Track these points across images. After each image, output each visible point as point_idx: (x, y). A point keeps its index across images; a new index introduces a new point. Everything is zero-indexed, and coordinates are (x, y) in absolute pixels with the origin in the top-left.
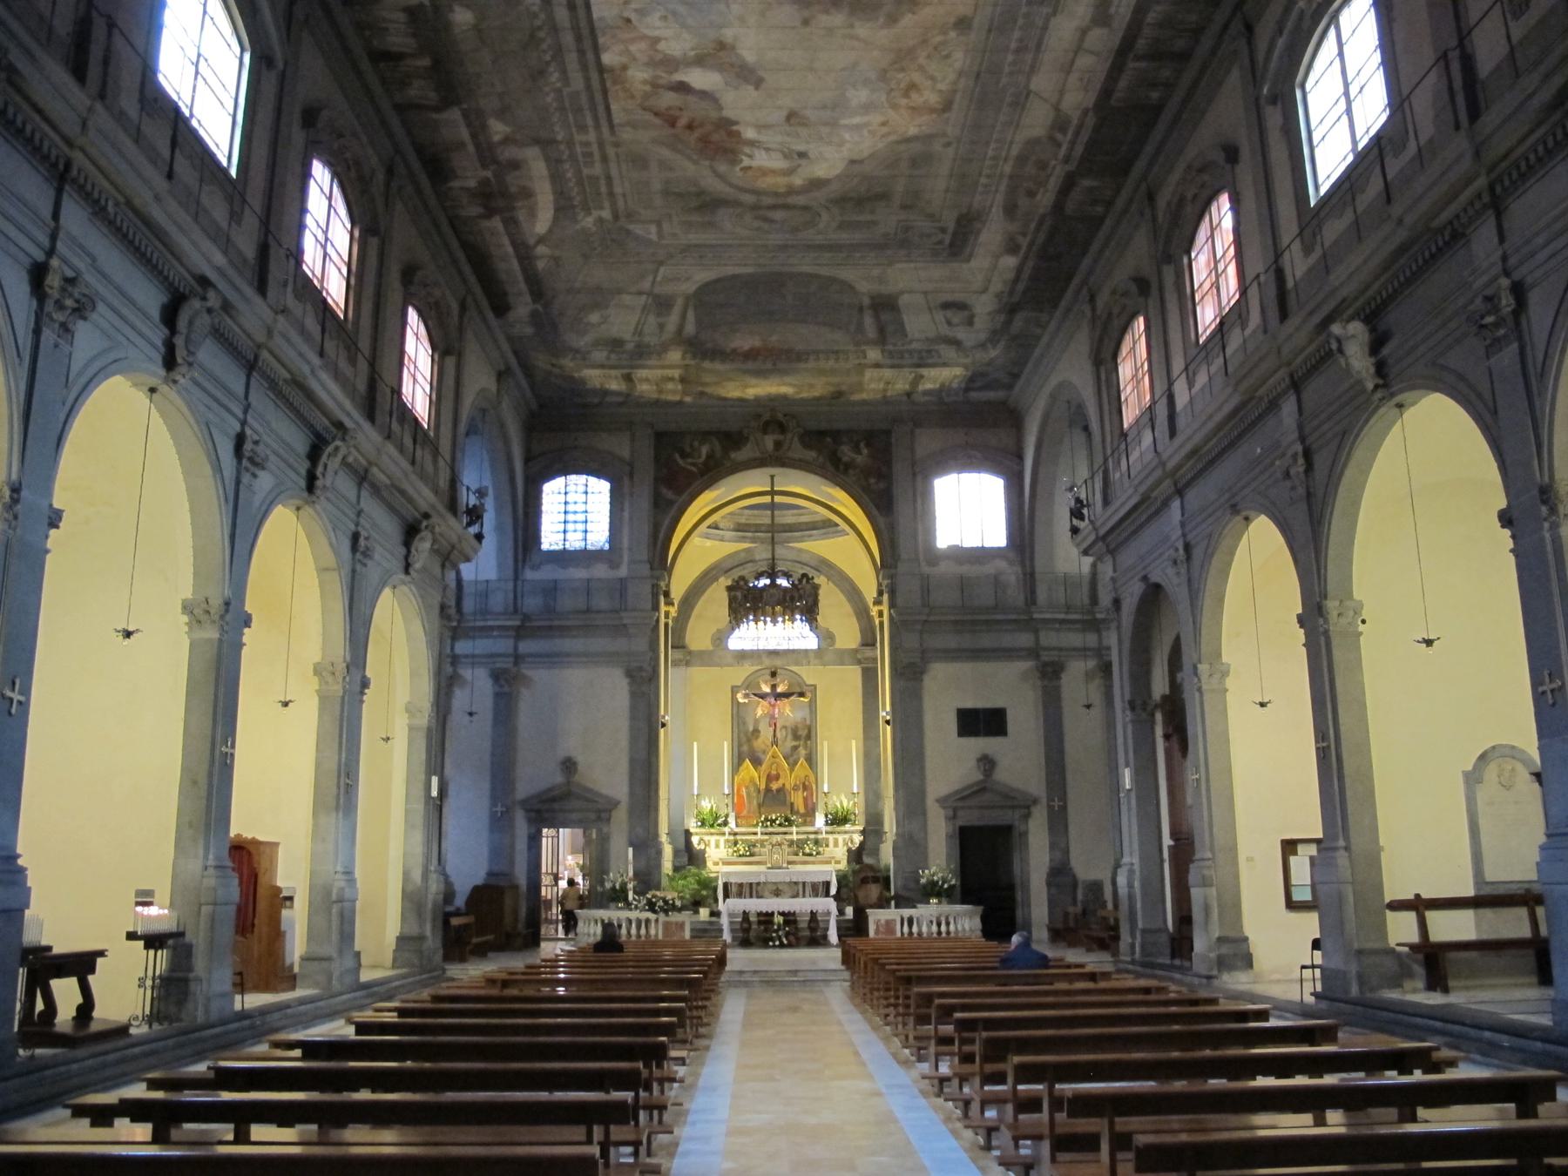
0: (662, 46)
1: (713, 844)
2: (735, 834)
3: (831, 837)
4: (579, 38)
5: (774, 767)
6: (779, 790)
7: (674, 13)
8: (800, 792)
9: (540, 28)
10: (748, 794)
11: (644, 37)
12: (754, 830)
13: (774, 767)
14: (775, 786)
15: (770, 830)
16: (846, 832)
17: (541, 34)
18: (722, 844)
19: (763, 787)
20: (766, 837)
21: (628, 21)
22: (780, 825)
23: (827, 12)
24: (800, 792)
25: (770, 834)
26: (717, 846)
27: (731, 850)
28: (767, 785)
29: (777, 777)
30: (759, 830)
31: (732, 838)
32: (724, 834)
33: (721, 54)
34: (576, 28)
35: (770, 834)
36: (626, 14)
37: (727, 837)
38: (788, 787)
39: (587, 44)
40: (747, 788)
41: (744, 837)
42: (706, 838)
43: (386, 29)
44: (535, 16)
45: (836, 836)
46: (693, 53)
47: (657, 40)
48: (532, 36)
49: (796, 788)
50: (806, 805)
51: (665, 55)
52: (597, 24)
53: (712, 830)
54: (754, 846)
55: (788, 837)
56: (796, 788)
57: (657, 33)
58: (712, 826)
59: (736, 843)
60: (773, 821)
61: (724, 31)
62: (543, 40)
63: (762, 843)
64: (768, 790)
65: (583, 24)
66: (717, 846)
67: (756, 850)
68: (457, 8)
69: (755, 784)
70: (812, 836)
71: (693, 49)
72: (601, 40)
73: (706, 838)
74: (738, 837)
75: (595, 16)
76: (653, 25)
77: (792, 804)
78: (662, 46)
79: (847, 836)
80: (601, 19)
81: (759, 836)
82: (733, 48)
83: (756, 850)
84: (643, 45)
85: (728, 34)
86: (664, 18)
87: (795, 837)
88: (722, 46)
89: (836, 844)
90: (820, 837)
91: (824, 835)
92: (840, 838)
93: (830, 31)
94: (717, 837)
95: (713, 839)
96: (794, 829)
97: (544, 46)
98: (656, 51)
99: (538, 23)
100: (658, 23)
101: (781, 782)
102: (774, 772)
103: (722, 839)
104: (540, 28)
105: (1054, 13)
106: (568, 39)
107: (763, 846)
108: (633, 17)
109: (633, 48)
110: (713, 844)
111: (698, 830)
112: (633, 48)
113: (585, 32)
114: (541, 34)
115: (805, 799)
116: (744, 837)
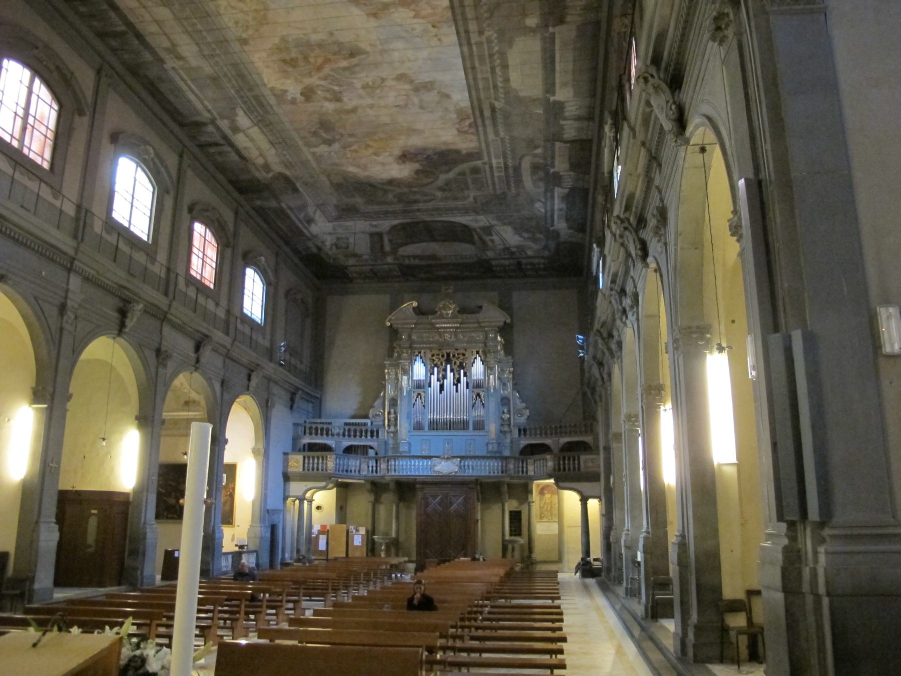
0: (412, 14)
4: (463, 14)
7: (407, 32)
9: (487, 19)
11: (423, 18)
17: (486, 15)
21: (434, 26)
23: (323, 41)
33: (375, 11)
34: (465, 20)
36: (436, 30)
39: (458, 11)
43: (581, 9)
44: (489, 26)
46: (392, 10)
47: (415, 17)
48: (492, 15)
51: (409, 8)
52: (453, 22)
57: (416, 21)
61: (375, 25)
62: (486, 12)
65: (460, 23)
68: (534, 26)
71: (392, 12)
72: (450, 14)
75: (454, 27)
76: (419, 25)
78: (412, 14)
80: (450, 27)
82: (368, 15)
84: (423, 13)
85: (373, 23)
86: (413, 29)
88: (375, 15)
93: (315, 31)
97: (485, 8)
98: (414, 10)
99: (487, 22)
100: (417, 26)
104: (487, 19)
105: (201, 51)
106: (470, 13)
108: (432, 29)
109: (430, 11)
112: (430, 11)
113: (459, 17)
114: (486, 15)
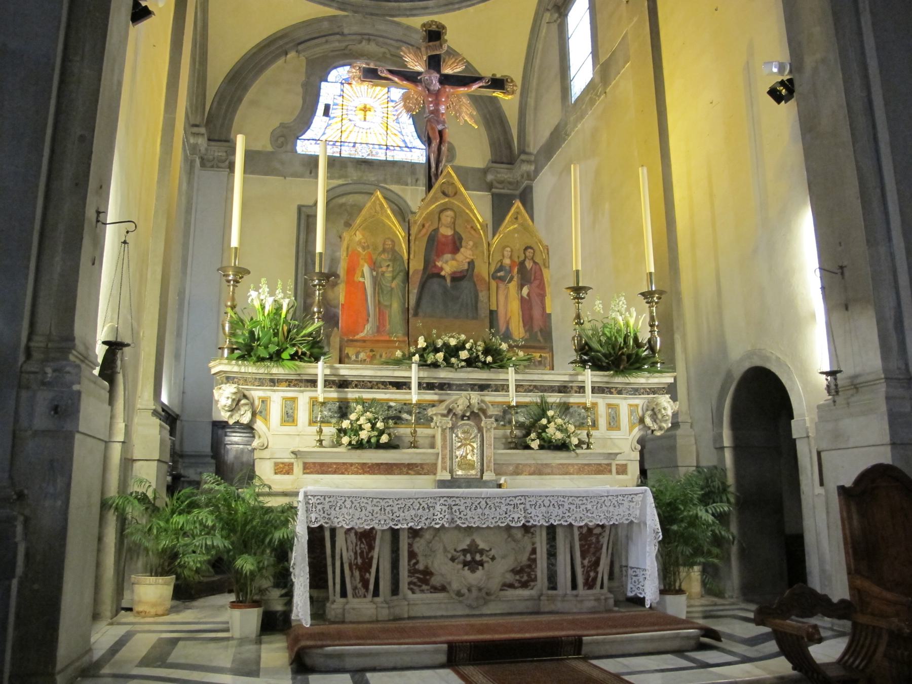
1: (276, 411)
2: (343, 384)
3: (602, 402)
5: (448, 217)
6: (457, 278)
8: (513, 286)
10: (377, 282)
12: (399, 373)
13: (448, 217)
14: (448, 265)
15: (444, 374)
16: (636, 391)
18: (303, 414)
19: (417, 265)
20: (430, 396)
22: (471, 363)
24: (513, 286)
25: (443, 386)
26: (289, 417)
27: (329, 431)
28: (427, 262)
29: (455, 245)
30: (414, 374)
31: (333, 394)
32: (313, 383)
35: (443, 386)
37: (321, 393)
38: (483, 270)
40: (374, 266)
41: (368, 395)
42: (257, 394)
45: (614, 399)
49: (500, 275)
50: (528, 320)
53: (276, 370)
54: (398, 419)
55: (491, 397)
56: (500, 275)
58: (276, 357)
59: (343, 411)
60: (452, 352)
63: (422, 416)
64: (431, 274)
66: (289, 417)
67: (404, 431)
69: (395, 257)
70: (554, 398)
73: (257, 394)
74: (352, 394)
77: (493, 315)
79: (640, 401)
81: (414, 396)
83: (404, 431)
87: (513, 398)
89: (614, 423)
90: (574, 399)
91: (589, 398)
92: (624, 404)
94: (291, 393)
95: (276, 398)
96: (511, 376)
101: (465, 255)
102: (447, 232)
103: (303, 398)
107: (424, 420)
110: (276, 411)
111: (233, 367)
115: (526, 304)
116: (368, 395)
